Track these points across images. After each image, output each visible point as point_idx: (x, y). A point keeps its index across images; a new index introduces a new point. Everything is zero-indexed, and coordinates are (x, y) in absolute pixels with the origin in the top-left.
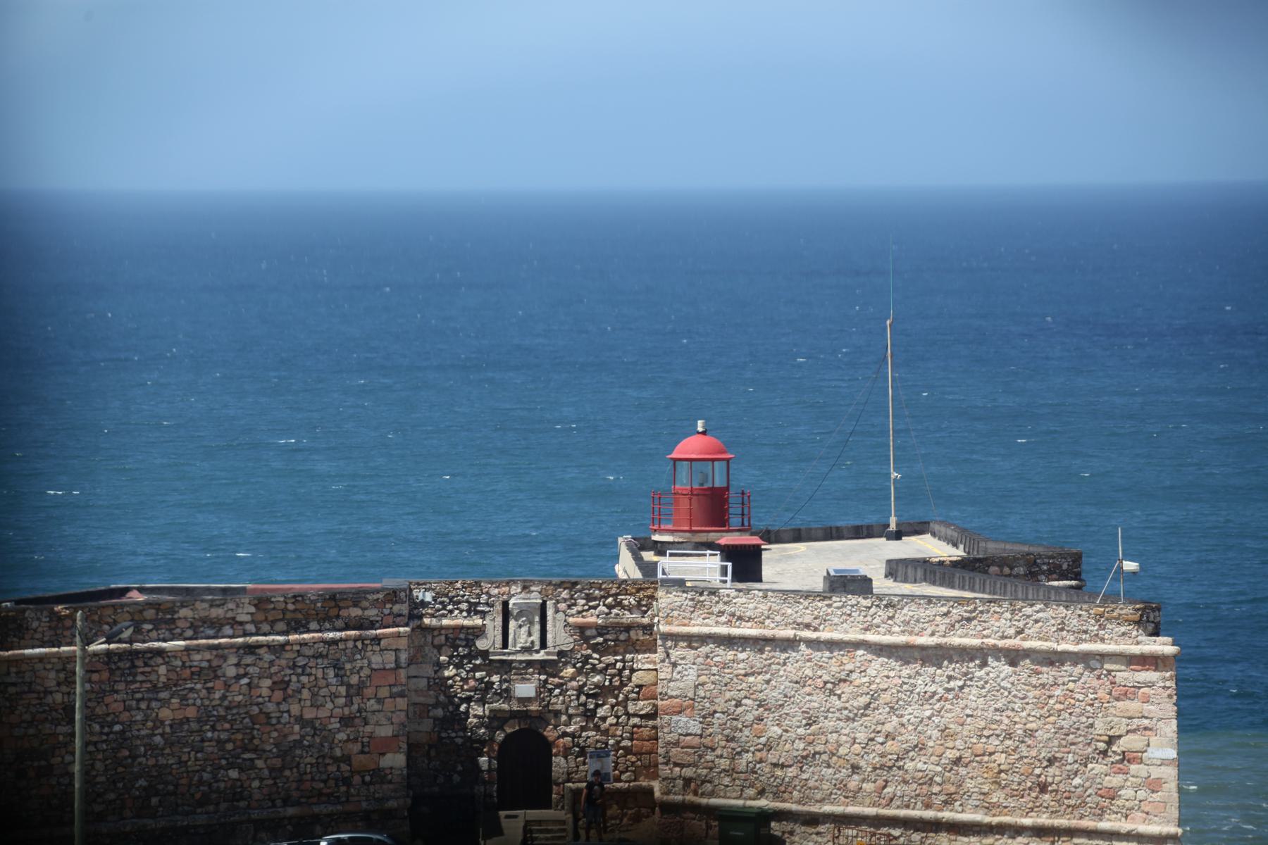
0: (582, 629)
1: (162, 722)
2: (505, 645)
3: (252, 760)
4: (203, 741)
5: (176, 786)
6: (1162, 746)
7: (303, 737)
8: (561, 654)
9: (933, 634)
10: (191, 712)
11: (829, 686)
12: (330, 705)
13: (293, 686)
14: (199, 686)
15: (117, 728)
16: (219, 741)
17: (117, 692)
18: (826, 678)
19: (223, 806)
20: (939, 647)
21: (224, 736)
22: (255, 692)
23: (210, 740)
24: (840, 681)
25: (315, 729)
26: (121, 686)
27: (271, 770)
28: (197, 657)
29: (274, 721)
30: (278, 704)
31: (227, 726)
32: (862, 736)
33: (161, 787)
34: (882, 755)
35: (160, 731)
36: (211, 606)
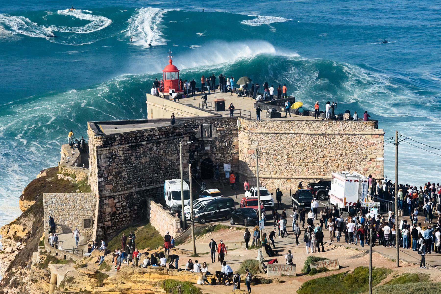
10: (148, 160)
13: (167, 151)
14: (149, 153)
15: (134, 165)
16: (154, 167)
18: (293, 143)
21: (154, 165)
22: (160, 154)
32: (302, 157)
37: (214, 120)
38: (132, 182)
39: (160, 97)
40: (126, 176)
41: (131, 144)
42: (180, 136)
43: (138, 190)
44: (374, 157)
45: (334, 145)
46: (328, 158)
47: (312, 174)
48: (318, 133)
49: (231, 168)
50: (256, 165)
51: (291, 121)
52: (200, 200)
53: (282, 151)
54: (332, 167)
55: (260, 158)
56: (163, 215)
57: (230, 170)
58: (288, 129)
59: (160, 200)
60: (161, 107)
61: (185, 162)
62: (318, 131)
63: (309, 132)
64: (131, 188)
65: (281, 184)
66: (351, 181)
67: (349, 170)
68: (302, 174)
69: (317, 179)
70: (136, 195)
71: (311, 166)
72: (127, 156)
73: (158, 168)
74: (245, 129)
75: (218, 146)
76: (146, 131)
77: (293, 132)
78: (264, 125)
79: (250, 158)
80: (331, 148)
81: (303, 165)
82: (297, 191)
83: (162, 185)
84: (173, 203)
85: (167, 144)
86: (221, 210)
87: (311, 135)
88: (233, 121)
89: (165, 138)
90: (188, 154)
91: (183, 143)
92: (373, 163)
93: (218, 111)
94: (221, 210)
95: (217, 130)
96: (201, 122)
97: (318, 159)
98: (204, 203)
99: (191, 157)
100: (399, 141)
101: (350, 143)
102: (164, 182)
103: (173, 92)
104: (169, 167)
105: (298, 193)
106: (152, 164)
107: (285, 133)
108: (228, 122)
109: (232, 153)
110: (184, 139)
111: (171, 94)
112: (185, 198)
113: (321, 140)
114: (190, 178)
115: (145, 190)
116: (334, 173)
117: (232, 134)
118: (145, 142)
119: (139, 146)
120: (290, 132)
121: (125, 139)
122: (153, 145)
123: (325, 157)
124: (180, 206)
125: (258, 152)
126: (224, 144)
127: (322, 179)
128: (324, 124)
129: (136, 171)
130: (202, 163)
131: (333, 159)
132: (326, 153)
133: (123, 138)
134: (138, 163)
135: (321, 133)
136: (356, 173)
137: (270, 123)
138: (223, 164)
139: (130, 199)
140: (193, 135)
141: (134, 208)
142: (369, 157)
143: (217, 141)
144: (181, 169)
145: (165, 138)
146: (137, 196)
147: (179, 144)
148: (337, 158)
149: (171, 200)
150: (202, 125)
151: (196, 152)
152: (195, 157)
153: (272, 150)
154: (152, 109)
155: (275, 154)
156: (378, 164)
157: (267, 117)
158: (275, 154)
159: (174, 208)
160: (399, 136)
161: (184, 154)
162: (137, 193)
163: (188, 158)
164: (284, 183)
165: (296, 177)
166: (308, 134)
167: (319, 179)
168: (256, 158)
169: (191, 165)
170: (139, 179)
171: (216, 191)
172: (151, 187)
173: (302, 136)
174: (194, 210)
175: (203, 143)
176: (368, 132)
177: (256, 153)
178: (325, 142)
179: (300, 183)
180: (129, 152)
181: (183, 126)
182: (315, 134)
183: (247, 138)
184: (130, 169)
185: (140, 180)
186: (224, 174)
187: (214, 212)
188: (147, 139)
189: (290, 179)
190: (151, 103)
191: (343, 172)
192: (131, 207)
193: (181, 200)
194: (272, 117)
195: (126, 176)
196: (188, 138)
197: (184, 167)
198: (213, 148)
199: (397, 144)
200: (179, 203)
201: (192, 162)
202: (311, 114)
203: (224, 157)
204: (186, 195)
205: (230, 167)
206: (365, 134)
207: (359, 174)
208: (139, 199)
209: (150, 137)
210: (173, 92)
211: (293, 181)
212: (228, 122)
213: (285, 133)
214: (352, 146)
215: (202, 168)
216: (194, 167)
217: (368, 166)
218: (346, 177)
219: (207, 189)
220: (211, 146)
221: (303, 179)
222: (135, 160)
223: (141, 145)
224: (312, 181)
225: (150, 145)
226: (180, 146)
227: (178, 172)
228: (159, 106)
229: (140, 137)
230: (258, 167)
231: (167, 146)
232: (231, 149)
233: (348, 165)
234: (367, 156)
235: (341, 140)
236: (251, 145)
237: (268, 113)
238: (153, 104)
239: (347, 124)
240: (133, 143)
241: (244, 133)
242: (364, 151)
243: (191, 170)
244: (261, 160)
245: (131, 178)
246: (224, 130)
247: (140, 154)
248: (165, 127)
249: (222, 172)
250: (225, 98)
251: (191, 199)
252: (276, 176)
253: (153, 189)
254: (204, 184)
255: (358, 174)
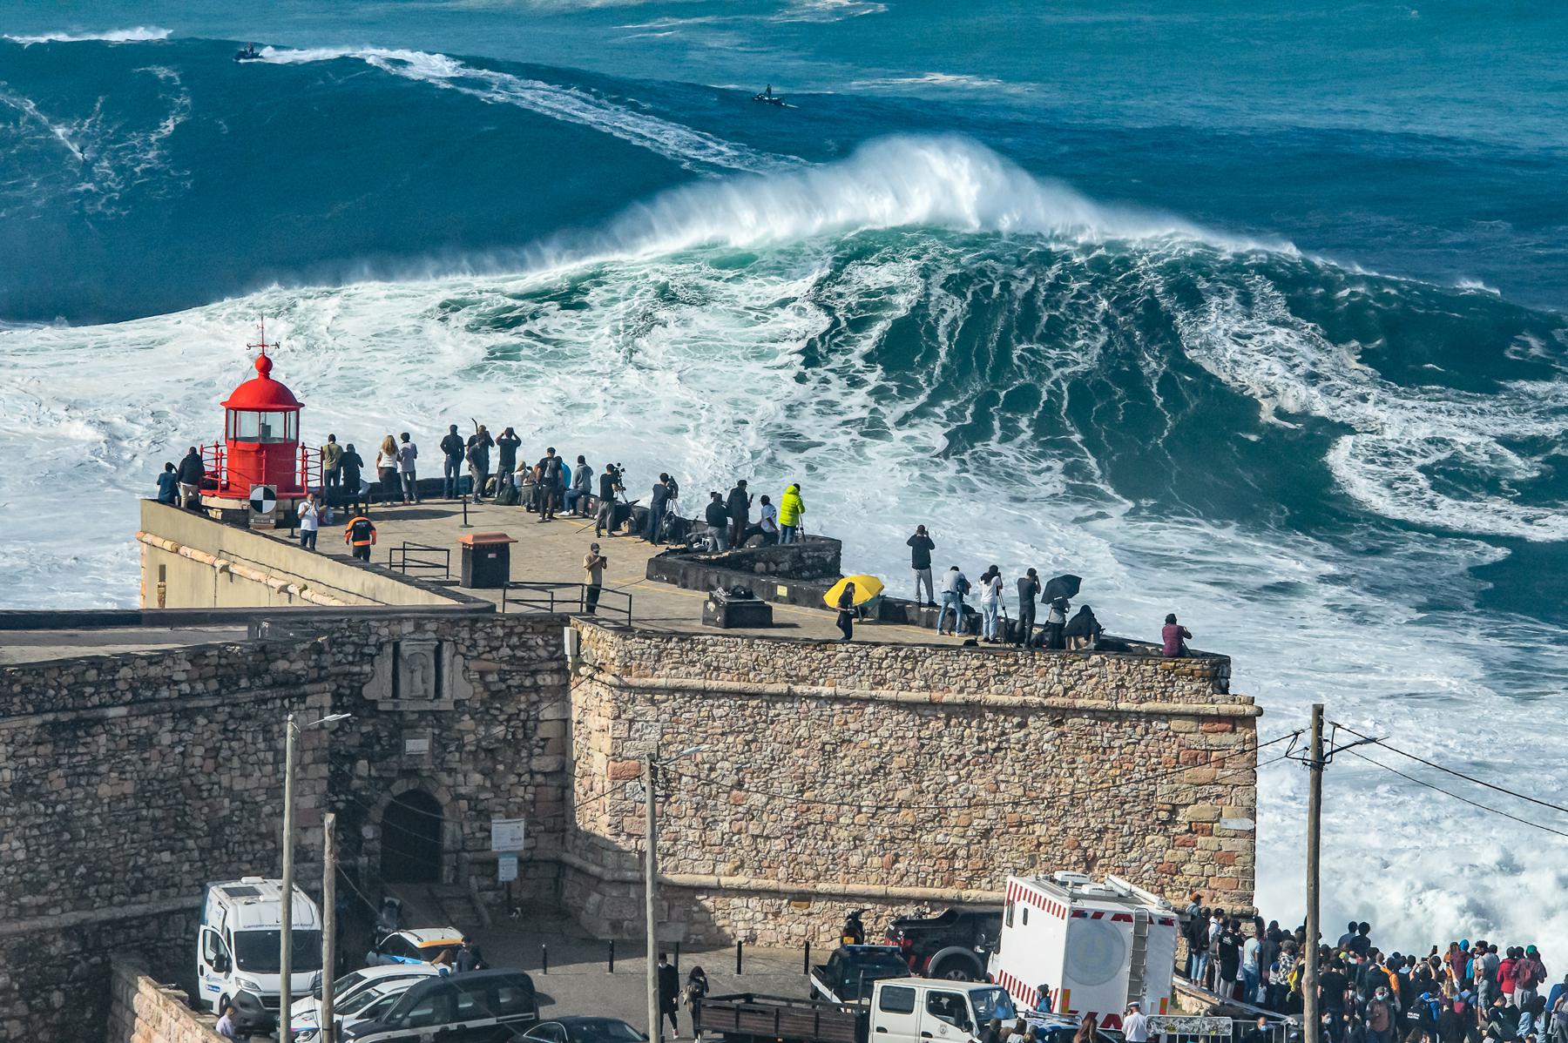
0: (482, 674)
1: (101, 800)
2: (395, 694)
3: (182, 840)
4: (138, 820)
5: (114, 872)
6: (1236, 816)
7: (232, 812)
8: (458, 703)
9: (961, 691)
10: (128, 788)
11: (828, 748)
12: (257, 774)
13: (224, 753)
14: (135, 758)
15: (60, 808)
17: (59, 767)
18: (826, 738)
19: (156, 893)
20: (967, 704)
21: (158, 813)
22: (188, 762)
23: (146, 819)
24: (843, 741)
25: (243, 802)
26: (64, 760)
27: (201, 850)
28: (136, 724)
29: (205, 794)
30: (209, 774)
31: (161, 802)
32: (868, 803)
33: (99, 874)
34: (892, 827)
35: (98, 810)
36: (150, 664)
37: (455, 623)
38: (46, 884)
39: (207, 517)
40: (21, 855)
41: (50, 717)
42: (292, 688)
43: (71, 918)
44: (1209, 816)
45: (1022, 755)
46: (990, 812)
47: (912, 879)
48: (947, 698)
49: (527, 835)
50: (648, 832)
51: (820, 643)
52: (369, 974)
53: (774, 774)
54: (1005, 852)
55: (667, 797)
56: (188, 1035)
57: (520, 845)
58: (804, 679)
59: (178, 974)
60: (209, 559)
61: (309, 802)
62: (947, 689)
63: (905, 695)
64: (41, 910)
65: (759, 916)
66: (1098, 915)
67: (1089, 868)
68: (862, 876)
69: (934, 902)
70: (60, 944)
71: (908, 845)
72: (28, 768)
73: (177, 827)
74: (599, 669)
75: (469, 738)
76: (128, 659)
77: (826, 691)
78: (694, 656)
79: (618, 796)
80: (1006, 765)
81: (868, 836)
82: (835, 953)
83: (188, 902)
84: (237, 982)
85: (225, 723)
86: (470, 1024)
87: (911, 706)
88: (544, 633)
89: (217, 693)
90: (324, 770)
91: (302, 718)
92: (1201, 839)
93: (476, 584)
94: (470, 1024)
95: (466, 669)
96: (396, 628)
97: (940, 817)
98: (386, 988)
99: (338, 782)
100: (1327, 748)
101: (1094, 750)
102: (204, 891)
103: (268, 495)
104: (228, 821)
105: (842, 959)
106: (148, 806)
107: (790, 696)
108: (520, 635)
109: (532, 773)
110: (309, 699)
111: (257, 506)
112: (298, 965)
113: (957, 731)
114: (328, 877)
115: (103, 923)
116: (1016, 880)
117: (536, 688)
118: (123, 711)
119: (88, 724)
120: (814, 689)
121: (26, 690)
122: (160, 723)
123: (973, 803)
124: (273, 1001)
125: (662, 779)
126: (499, 730)
127: (960, 901)
128: (976, 663)
129: (67, 836)
130: (391, 810)
131: (1015, 817)
132: (979, 785)
133: (17, 688)
134: (83, 801)
135: (960, 699)
136: (1121, 884)
137: (720, 649)
138: (489, 820)
139: (32, 960)
140: (352, 688)
141: (47, 1000)
142: (1183, 816)
143: (466, 717)
144: (286, 833)
145: (217, 693)
146: (67, 947)
147: (281, 722)
148: (1032, 812)
149: (229, 970)
150: (396, 646)
151: (362, 766)
152: (356, 783)
153: (727, 765)
154: (162, 569)
155: (739, 785)
156: (1227, 845)
157: (705, 621)
158: (739, 785)
159: (244, 1005)
160: (1327, 731)
161: (304, 769)
162: (66, 932)
163: (323, 786)
164: (776, 915)
165: (838, 888)
166: (896, 705)
167: (941, 901)
168: (647, 797)
169: (338, 819)
170: (82, 869)
171: (453, 936)
172: (138, 909)
173: (870, 709)
174: (337, 1017)
175: (400, 725)
176: (1181, 707)
177: (647, 777)
178: (980, 740)
179: (854, 919)
180: (42, 750)
181: (307, 646)
182: (931, 704)
183: (608, 709)
184: (39, 826)
185: (82, 876)
186: (493, 864)
187: (436, 1029)
188: (129, 696)
189: (803, 897)
190: (158, 542)
191: (1059, 876)
192: (35, 996)
193: (276, 970)
194: (728, 623)
195: (21, 855)
196: (327, 700)
197: (300, 827)
198: (445, 747)
199: (1318, 764)
200: (270, 983)
201: (341, 805)
202: (912, 615)
203: (496, 788)
204: (304, 950)
205: (521, 834)
206: (1169, 716)
207: (1134, 888)
208: (74, 962)
209: (148, 688)
210: (268, 495)
211: (816, 907)
212: (520, 635)
213: (790, 696)
214: (1108, 766)
215: (387, 834)
216: (348, 823)
217: (1181, 854)
218: (1074, 898)
219: (407, 928)
220: (436, 740)
221: (870, 898)
222: (70, 786)
223: (101, 721)
224: (910, 911)
225: (145, 722)
226: (289, 731)
227: (270, 846)
228: (199, 555)
229: (97, 685)
230: (654, 837)
231: (226, 730)
232: (531, 755)
233: (1085, 844)
234: (1174, 810)
235: (1051, 732)
236: (629, 739)
237: (711, 606)
238: (168, 545)
239: (1082, 665)
240: (65, 709)
241: (596, 688)
242: (1163, 788)
243: (335, 841)
244: (672, 810)
245: (44, 867)
246: (500, 672)
247: (95, 762)
248: (222, 650)
249: (481, 856)
250: (513, 532)
251: (324, 972)
252: (739, 880)
253: (143, 920)
254: (391, 904)
255: (1127, 886)
